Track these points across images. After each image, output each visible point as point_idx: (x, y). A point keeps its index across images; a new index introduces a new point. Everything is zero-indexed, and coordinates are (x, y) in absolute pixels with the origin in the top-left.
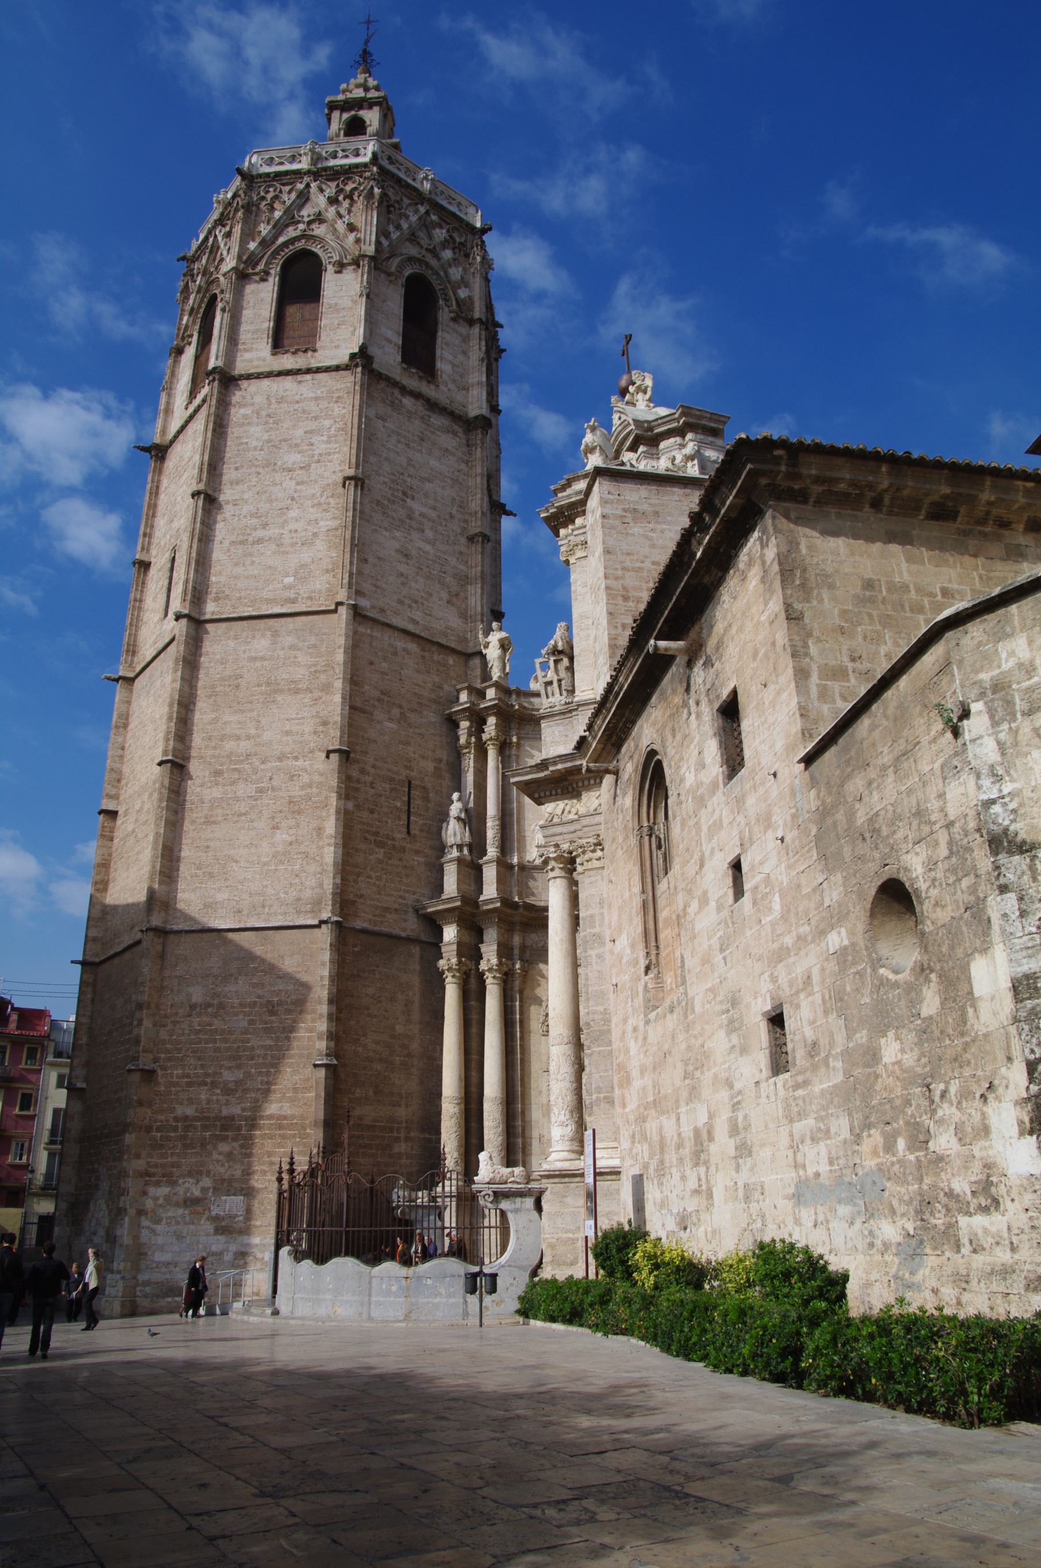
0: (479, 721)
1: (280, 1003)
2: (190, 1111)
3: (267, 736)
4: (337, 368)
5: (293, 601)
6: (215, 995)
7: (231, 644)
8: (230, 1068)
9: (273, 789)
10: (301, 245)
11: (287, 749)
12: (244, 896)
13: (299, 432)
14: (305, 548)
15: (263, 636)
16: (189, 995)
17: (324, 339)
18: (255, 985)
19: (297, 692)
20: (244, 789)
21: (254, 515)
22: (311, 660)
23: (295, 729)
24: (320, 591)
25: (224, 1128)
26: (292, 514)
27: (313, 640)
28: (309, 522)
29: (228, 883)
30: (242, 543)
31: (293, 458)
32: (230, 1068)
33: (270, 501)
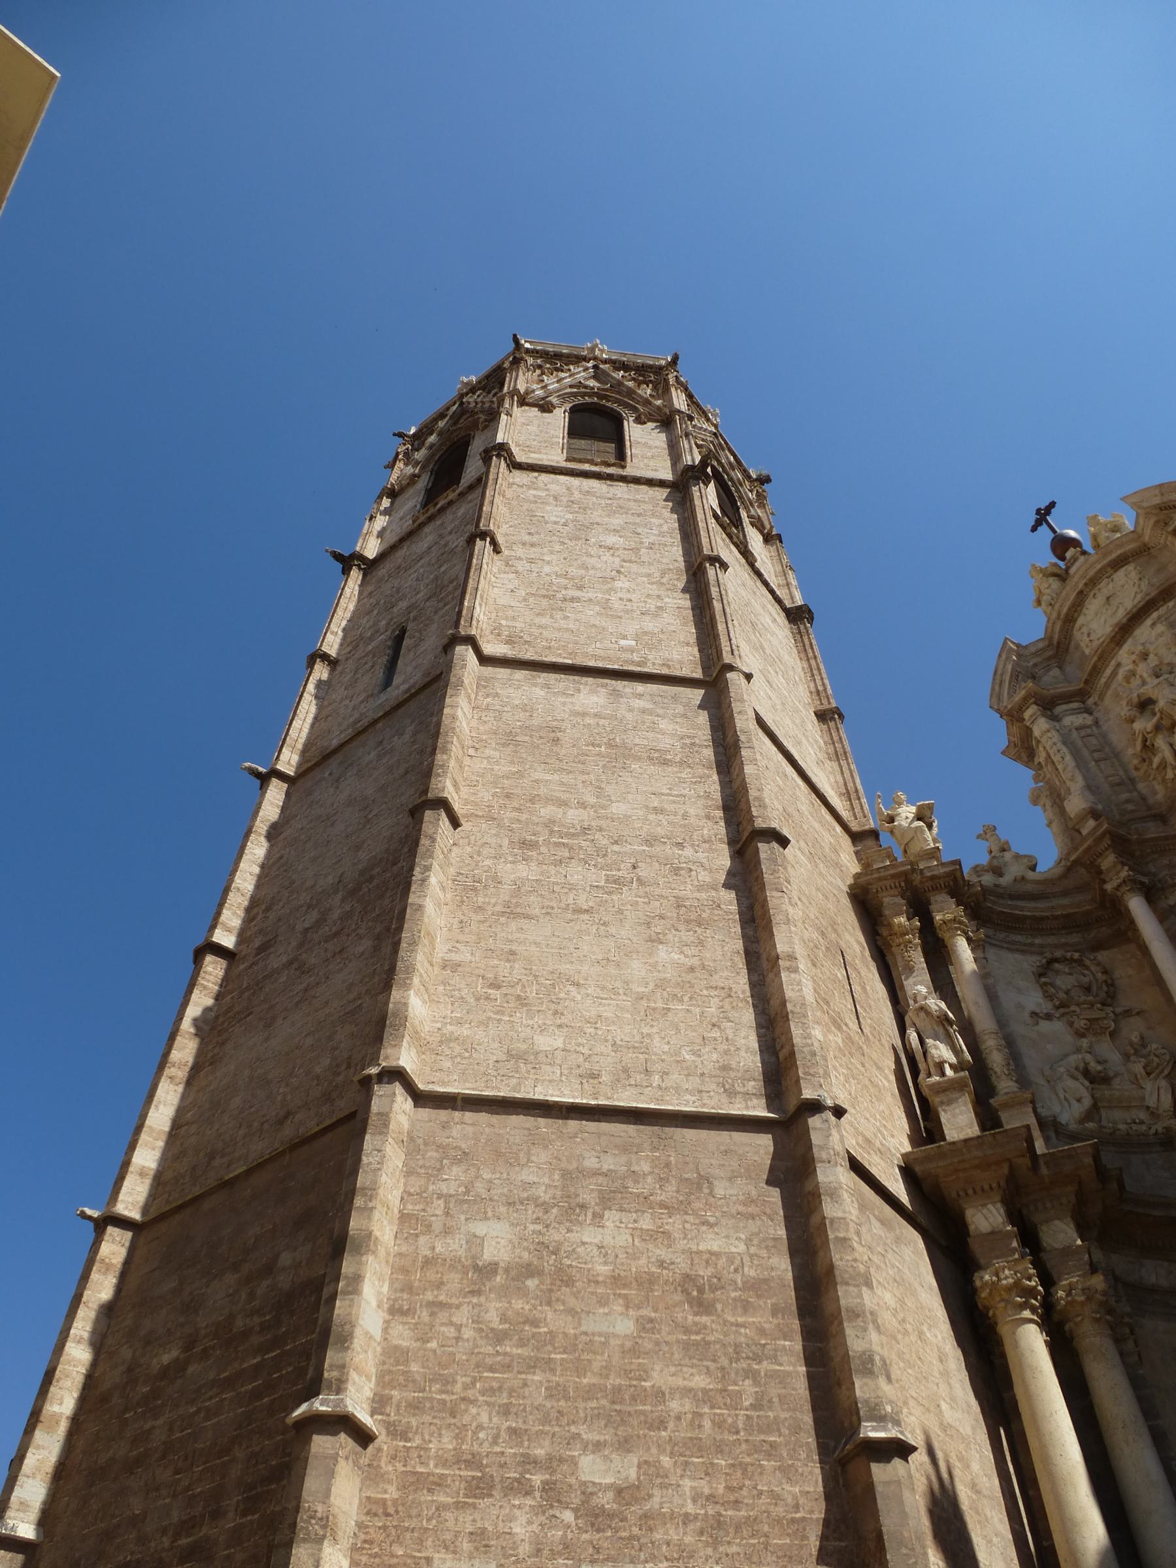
1: (718, 1284)
3: (618, 809)
5: (642, 664)
7: (539, 693)
8: (598, 1446)
12: (600, 1048)
14: (647, 618)
15: (593, 692)
16: (475, 1241)
18: (650, 1236)
19: (666, 763)
20: (576, 873)
22: (681, 730)
23: (670, 807)
24: (681, 662)
29: (564, 1020)
32: (598, 1446)
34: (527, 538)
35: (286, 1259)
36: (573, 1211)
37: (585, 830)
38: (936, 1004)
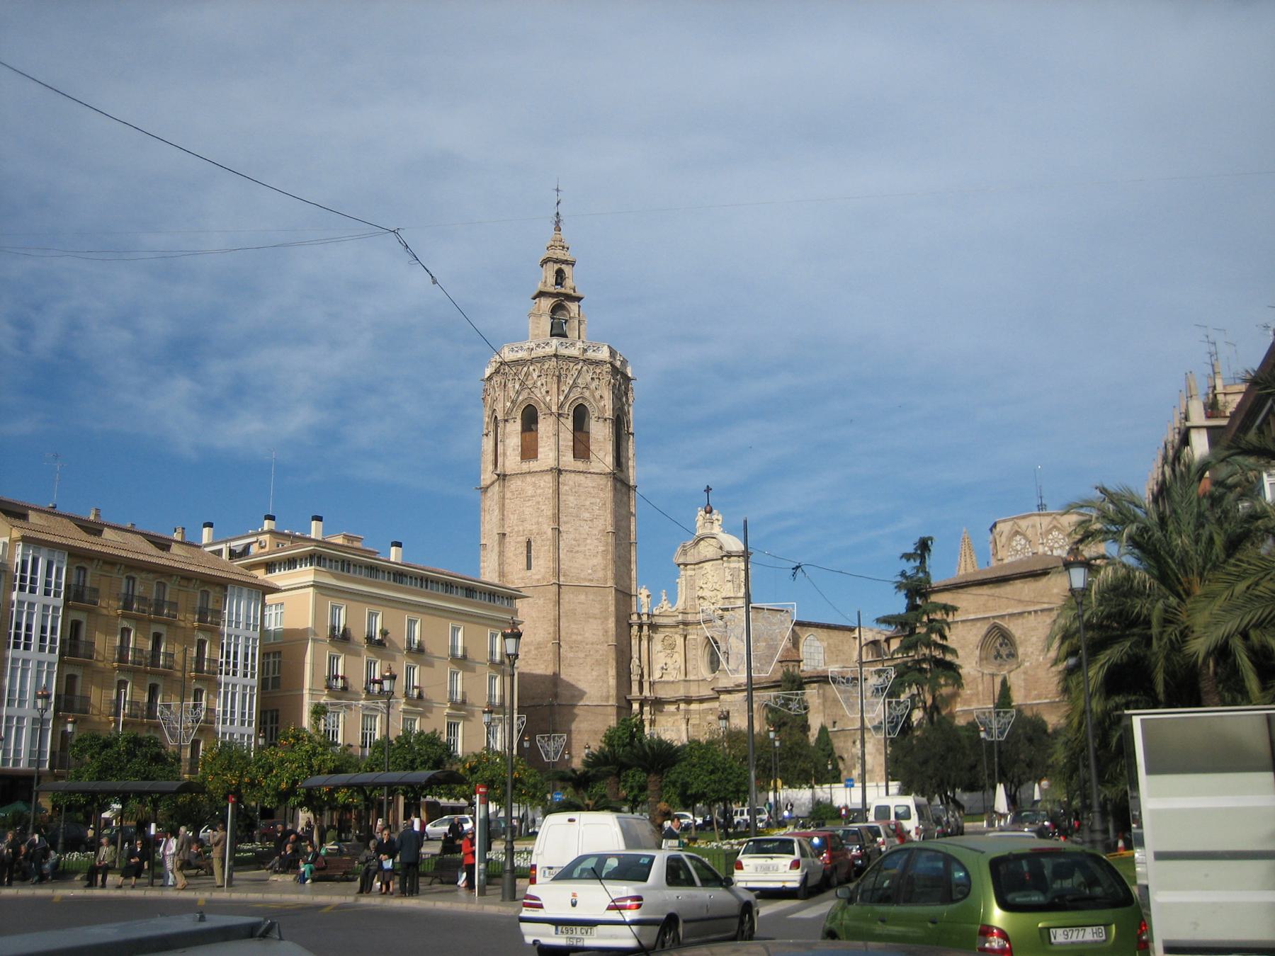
0: (641, 627)
10: (580, 401)
13: (588, 503)
31: (586, 515)
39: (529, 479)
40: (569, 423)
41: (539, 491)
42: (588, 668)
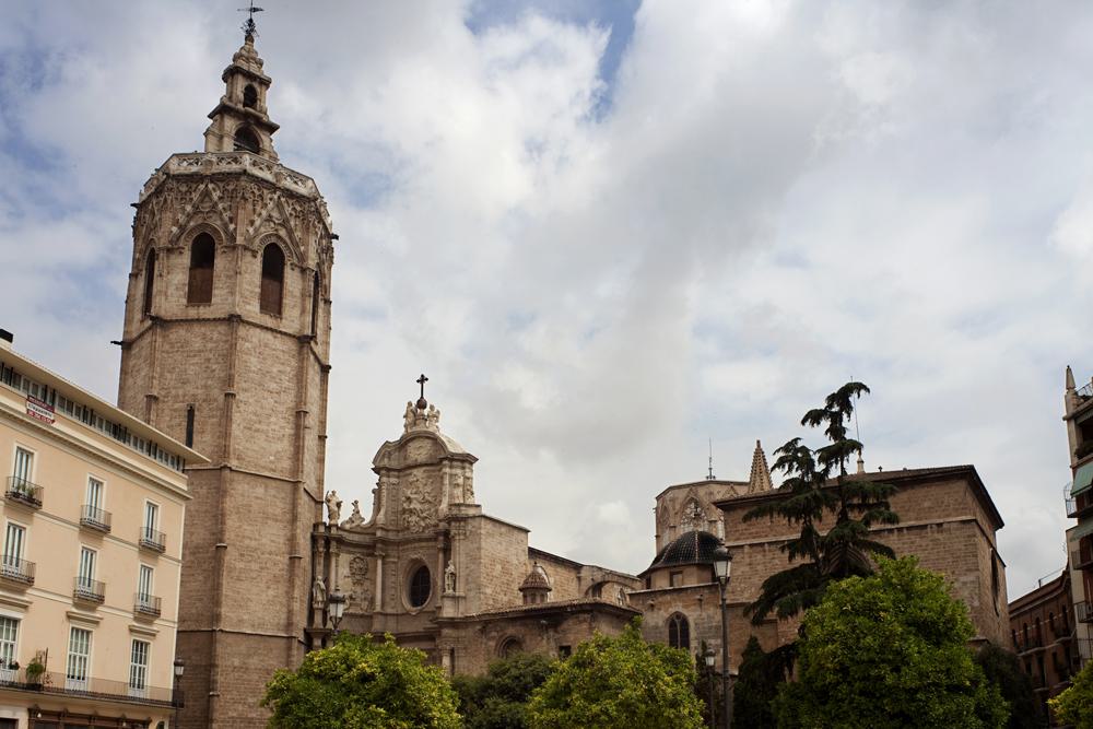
2: (235, 715)
3: (264, 541)
4: (294, 336)
6: (245, 663)
7: (246, 486)
9: (268, 568)
10: (273, 240)
11: (273, 549)
13: (275, 370)
17: (286, 312)
19: (277, 521)
21: (255, 414)
25: (249, 723)
26: (273, 419)
27: (283, 495)
28: (281, 427)
30: (250, 429)
31: (273, 386)
33: (262, 408)
34: (244, 385)
35: (193, 657)
36: (249, 656)
37: (256, 549)
38: (322, 583)
39: (197, 328)
40: (256, 266)
41: (210, 345)
42: (263, 585)
